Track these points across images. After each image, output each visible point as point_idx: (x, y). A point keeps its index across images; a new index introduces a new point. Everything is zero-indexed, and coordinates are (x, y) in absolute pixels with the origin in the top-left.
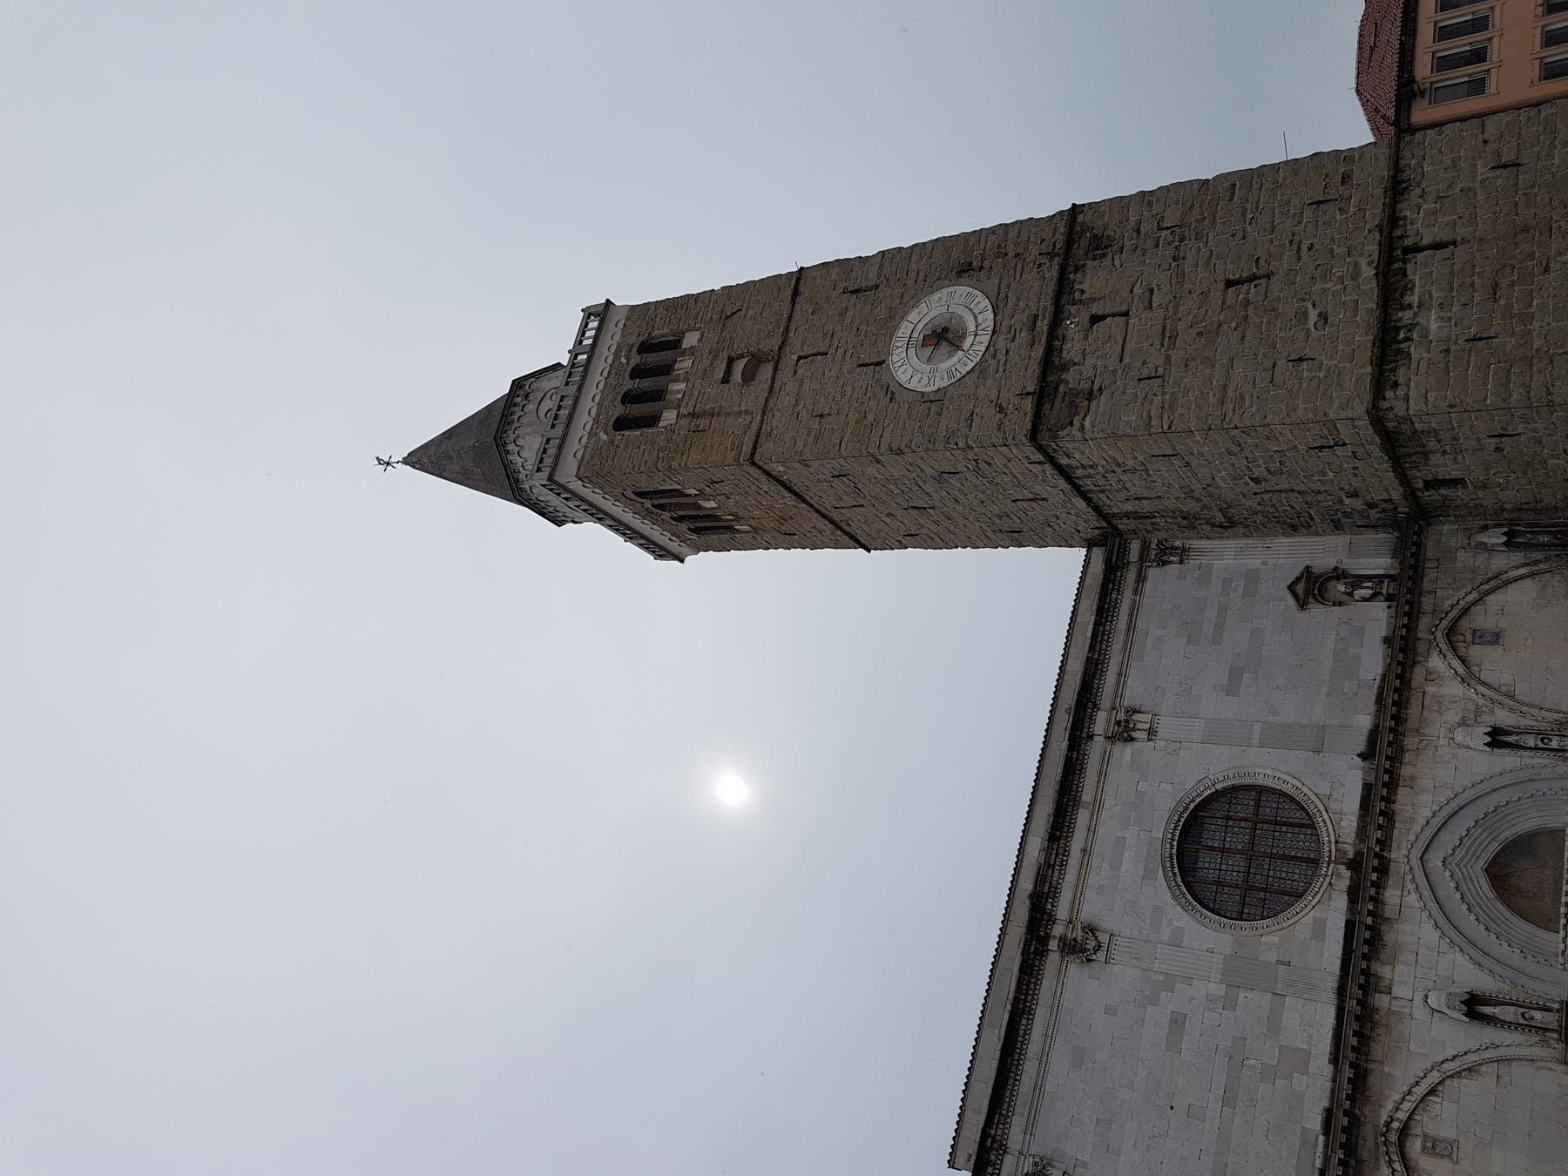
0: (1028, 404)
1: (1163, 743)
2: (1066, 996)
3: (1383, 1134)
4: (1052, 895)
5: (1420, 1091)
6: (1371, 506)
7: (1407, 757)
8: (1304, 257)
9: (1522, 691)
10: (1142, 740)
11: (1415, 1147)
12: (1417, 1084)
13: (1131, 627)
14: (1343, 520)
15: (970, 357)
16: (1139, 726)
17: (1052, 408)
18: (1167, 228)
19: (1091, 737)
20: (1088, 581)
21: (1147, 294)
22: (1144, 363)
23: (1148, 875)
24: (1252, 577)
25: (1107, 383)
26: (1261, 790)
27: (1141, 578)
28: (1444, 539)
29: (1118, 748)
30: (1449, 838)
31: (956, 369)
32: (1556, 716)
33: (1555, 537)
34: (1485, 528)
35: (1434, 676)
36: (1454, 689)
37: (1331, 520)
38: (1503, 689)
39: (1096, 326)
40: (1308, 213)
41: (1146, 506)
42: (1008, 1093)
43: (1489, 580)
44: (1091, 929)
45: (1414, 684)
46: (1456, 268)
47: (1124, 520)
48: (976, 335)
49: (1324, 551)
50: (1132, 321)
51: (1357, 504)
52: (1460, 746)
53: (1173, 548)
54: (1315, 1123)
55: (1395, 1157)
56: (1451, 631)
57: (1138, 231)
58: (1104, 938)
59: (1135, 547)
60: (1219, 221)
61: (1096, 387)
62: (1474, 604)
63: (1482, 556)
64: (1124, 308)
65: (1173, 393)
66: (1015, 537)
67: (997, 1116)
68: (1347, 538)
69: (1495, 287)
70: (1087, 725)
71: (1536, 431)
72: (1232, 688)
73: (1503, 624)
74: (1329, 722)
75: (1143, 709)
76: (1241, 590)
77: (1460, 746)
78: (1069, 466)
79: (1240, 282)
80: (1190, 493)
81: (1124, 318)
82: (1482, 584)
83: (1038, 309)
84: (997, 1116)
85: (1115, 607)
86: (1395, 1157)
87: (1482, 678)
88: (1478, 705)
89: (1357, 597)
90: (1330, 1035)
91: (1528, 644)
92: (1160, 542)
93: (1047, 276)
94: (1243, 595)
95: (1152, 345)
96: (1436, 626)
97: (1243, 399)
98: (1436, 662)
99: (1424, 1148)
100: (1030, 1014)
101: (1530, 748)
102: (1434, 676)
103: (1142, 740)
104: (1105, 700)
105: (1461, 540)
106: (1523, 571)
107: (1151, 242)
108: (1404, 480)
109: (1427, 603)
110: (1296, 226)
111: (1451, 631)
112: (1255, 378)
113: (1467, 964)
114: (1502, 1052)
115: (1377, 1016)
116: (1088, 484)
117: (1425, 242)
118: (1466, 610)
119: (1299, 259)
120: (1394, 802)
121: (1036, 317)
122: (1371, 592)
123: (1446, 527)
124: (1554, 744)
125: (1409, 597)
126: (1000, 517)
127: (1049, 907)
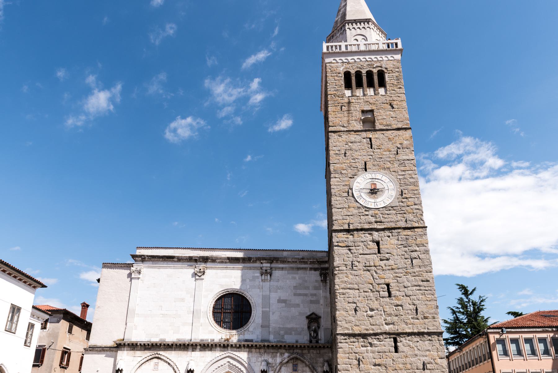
0: (346, 227)
3: (157, 353)
5: (168, 360)
15: (366, 202)
17: (344, 234)
18: (412, 261)
21: (386, 258)
22: (359, 262)
25: (352, 251)
31: (361, 198)
39: (375, 243)
48: (375, 203)
50: (375, 255)
57: (412, 252)
61: (350, 248)
64: (381, 252)
65: (346, 273)
79: (388, 289)
81: (377, 253)
93: (397, 223)
95: (365, 263)
97: (344, 294)
107: (407, 256)
112: (351, 297)
115: (186, 349)
120: (244, 348)
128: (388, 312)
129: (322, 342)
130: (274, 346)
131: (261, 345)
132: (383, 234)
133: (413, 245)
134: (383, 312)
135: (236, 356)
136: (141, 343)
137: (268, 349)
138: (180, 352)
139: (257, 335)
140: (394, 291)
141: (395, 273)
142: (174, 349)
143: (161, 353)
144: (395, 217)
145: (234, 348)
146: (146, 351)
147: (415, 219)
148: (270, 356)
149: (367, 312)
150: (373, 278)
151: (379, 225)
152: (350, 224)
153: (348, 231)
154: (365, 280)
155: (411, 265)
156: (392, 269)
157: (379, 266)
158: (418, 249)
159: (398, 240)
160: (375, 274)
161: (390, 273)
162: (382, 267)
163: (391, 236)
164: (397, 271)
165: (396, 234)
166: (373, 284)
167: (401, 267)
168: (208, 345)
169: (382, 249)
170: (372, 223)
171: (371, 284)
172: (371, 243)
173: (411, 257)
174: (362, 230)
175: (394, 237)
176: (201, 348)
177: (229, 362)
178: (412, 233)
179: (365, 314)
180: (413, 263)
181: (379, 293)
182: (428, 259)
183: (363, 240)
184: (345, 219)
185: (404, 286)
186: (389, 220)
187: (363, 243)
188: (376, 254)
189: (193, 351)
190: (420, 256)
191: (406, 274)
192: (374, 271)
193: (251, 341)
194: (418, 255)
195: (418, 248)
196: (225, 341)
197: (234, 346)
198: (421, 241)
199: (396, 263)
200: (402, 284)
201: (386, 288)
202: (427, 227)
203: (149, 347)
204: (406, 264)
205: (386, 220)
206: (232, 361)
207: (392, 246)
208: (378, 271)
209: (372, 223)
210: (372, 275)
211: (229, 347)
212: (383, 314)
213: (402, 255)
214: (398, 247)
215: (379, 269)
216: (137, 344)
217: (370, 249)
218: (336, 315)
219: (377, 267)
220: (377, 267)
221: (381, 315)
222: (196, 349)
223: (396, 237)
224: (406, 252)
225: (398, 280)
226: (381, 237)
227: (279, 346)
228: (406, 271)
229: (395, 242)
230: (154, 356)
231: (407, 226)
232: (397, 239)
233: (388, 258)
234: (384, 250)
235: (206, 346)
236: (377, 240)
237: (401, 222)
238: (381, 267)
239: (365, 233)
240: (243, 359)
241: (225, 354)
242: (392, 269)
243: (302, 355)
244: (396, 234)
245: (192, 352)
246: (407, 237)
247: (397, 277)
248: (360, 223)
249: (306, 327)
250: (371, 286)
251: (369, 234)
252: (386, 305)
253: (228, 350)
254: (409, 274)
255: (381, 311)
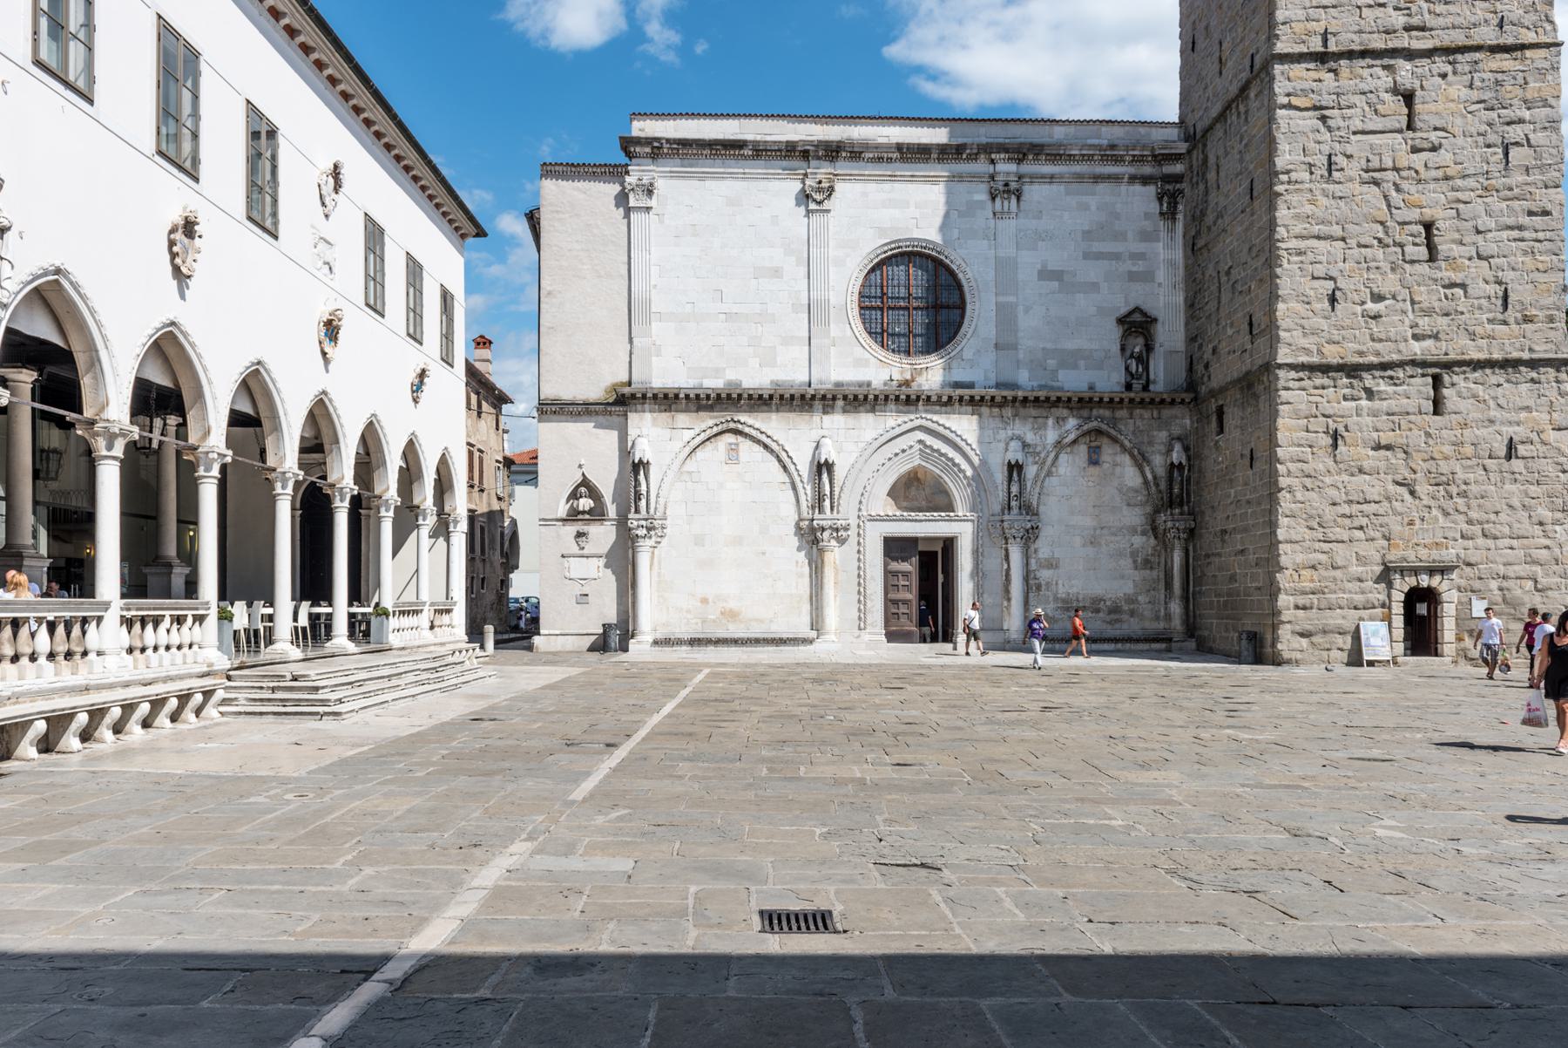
1: (992, 225)
2: (777, 183)
4: (853, 155)
5: (763, 438)
6: (1207, 366)
7: (996, 410)
8: (1446, 291)
9: (1053, 480)
10: (994, 207)
11: (730, 438)
12: (768, 437)
13: (1097, 179)
14: (1196, 345)
16: (1006, 203)
18: (1506, 154)
19: (993, 162)
20: (1142, 130)
21: (1430, 145)
23: (881, 231)
24: (1147, 277)
26: (962, 307)
27: (1145, 180)
28: (1177, 421)
29: (984, 187)
30: (937, 444)
32: (1035, 503)
33: (1177, 496)
34: (1186, 449)
35: (1061, 423)
36: (1051, 436)
37: (1196, 336)
38: (1054, 469)
39: (1400, 98)
40: (1500, 290)
41: (1211, 176)
42: (695, 152)
43: (1143, 456)
44: (831, 190)
45: (1052, 410)
46: (1412, 418)
47: (1201, 156)
49: (1171, 334)
50: (1399, 136)
51: (1208, 355)
52: (1007, 444)
53: (1176, 203)
54: (732, 375)
55: (720, 427)
56: (1099, 432)
58: (826, 205)
59: (1178, 168)
60: (1504, 205)
62: (1122, 446)
63: (1163, 448)
66: (1190, 47)
67: (675, 146)
68: (1183, 349)
69: (1388, 447)
70: (1002, 156)
71: (1254, 481)
72: (1045, 274)
73: (1106, 466)
74: (1021, 351)
75: (1022, 203)
76: (1135, 269)
77: (1007, 444)
78: (1247, 97)
80: (1220, 216)
81: (1405, 127)
82: (1139, 450)
83: (1431, 29)
84: (675, 146)
85: (1116, 161)
86: (720, 427)
87: (1061, 455)
88: (1039, 454)
89: (1129, 361)
90: (789, 378)
91: (1090, 484)
92: (1181, 192)
94: (1130, 273)
95: (1368, 161)
96: (1102, 421)
98: (1072, 422)
99: (730, 444)
100: (758, 156)
101: (1009, 489)
102: (1061, 423)
103: (994, 207)
104: (1028, 168)
105: (1176, 431)
106: (1150, 476)
107: (1492, 138)
108: (1223, 390)
109: (1122, 413)
110: (1484, 280)
111: (1099, 432)
113: (852, 460)
114: (799, 486)
116: (1233, 118)
117: (1446, 392)
118: (1115, 440)
119: (1444, 287)
120: (961, 405)
121: (1423, 29)
122: (1134, 371)
123: (1188, 422)
124: (1013, 503)
125: (1126, 400)
126: (1207, 28)
127: (844, 154)
128: (1425, 305)
129: (1159, 387)
130: (1042, 398)
131: (1005, 397)
132: (1427, 68)
133: (1515, 102)
134: (1408, 303)
135: (939, 425)
136: (688, 392)
137: (1025, 407)
138: (792, 415)
139: (986, 371)
140: (1446, 242)
141: (1453, 189)
142: (774, 408)
143: (743, 417)
144: (1468, 13)
145: (934, 404)
146: (702, 414)
147: (1529, 19)
148: (1029, 426)
149: (1363, 303)
150: (1389, 206)
151: (1418, 39)
152: (1329, 36)
153: (1322, 58)
154: (1365, 210)
155: (1501, 167)
156: (1447, 178)
157: (1410, 168)
158: (1527, 115)
159: (1471, 86)
160: (1394, 194)
161: (1439, 190)
162: (1417, 172)
163: (1450, 73)
164: (1459, 182)
165: (1467, 68)
166: (1388, 224)
167: (1471, 171)
168: (866, 397)
169: (1421, 117)
170: (1395, 32)
171: (1382, 223)
172: (1387, 97)
173: (1506, 141)
174: (1364, 54)
175: (1458, 78)
176: (846, 405)
177: (920, 442)
178: (1517, 62)
179: (1359, 309)
180: (1510, 159)
181: (1403, 251)
182: (1553, 148)
183: (1366, 88)
184: (1313, 20)
185: (1477, 229)
186: (1449, 20)
187: (1363, 97)
188: (1400, 131)
189: (825, 412)
190: (1531, 136)
191: (1484, 194)
192: (1391, 184)
193: (971, 386)
194: (1526, 135)
195: (1528, 112)
196: (900, 386)
197: (934, 398)
198: (1540, 89)
199: (1458, 161)
200: (1471, 224)
201: (1424, 235)
202: (1559, 45)
203: (710, 402)
204: (1488, 163)
205: (1441, 21)
206: (929, 440)
207: (1452, 105)
208: (1405, 185)
209: (1395, 32)
210: (1385, 197)
211: (921, 403)
212: (1410, 308)
213: (1479, 134)
214: (1470, 109)
215: (1407, 179)
216: (677, 396)
217: (1384, 116)
218: (1277, 313)
219: (1401, 173)
220: (1402, 173)
221: (1404, 312)
222: (833, 407)
223: (1465, 77)
224: (1490, 125)
225: (1461, 211)
226: (1421, 78)
227: (1053, 398)
228: (1486, 183)
229: (1461, 94)
230: (725, 426)
231: (1501, 41)
232: (1468, 84)
233: (1436, 143)
234: (1426, 118)
235: (858, 400)
236: (1408, 86)
237: (1484, 29)
238: (1413, 172)
239: (1373, 66)
240: (959, 433)
241: (912, 420)
242: (1447, 178)
243: (1114, 422)
244: (1467, 68)
245: (826, 418)
246: (1500, 77)
247: (1459, 201)
248: (1361, 32)
249: (1115, 348)
250: (1380, 228)
251: (1384, 67)
252: (1419, 285)
253: (917, 411)
254: (1495, 194)
255: (1405, 301)
